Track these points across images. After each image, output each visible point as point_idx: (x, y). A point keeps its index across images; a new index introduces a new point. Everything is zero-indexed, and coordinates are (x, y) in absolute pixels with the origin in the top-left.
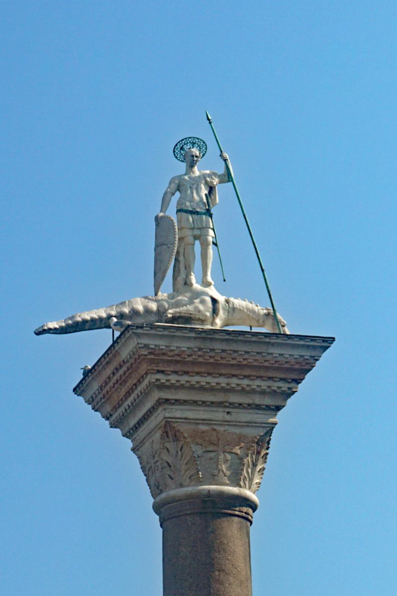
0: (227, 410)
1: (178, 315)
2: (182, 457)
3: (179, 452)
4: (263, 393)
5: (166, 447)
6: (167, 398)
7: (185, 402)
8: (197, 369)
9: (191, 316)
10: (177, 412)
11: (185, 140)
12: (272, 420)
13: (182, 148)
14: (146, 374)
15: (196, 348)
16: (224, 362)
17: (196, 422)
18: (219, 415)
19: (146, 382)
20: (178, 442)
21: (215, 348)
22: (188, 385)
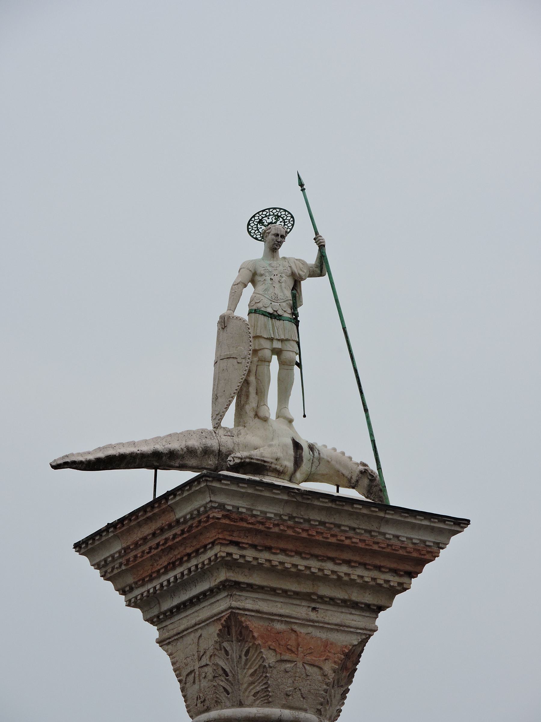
0: (313, 605)
1: (248, 460)
2: (246, 664)
3: (244, 658)
4: (364, 586)
5: (224, 648)
6: (237, 580)
7: (261, 589)
8: (282, 545)
9: (266, 464)
10: (247, 602)
11: (267, 211)
12: (371, 627)
13: (261, 222)
14: (213, 543)
15: (286, 516)
16: (320, 538)
17: (271, 617)
18: (301, 611)
19: (210, 554)
20: (244, 643)
21: (311, 518)
22: (267, 565)
